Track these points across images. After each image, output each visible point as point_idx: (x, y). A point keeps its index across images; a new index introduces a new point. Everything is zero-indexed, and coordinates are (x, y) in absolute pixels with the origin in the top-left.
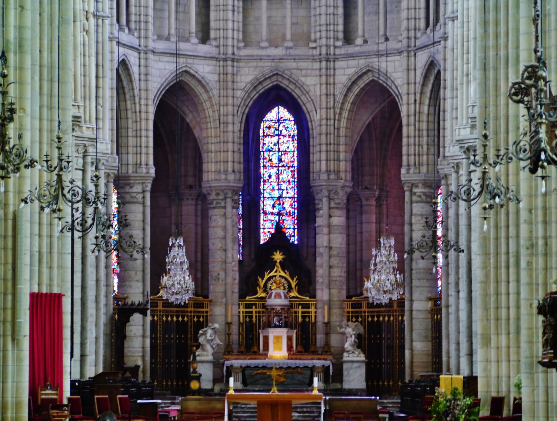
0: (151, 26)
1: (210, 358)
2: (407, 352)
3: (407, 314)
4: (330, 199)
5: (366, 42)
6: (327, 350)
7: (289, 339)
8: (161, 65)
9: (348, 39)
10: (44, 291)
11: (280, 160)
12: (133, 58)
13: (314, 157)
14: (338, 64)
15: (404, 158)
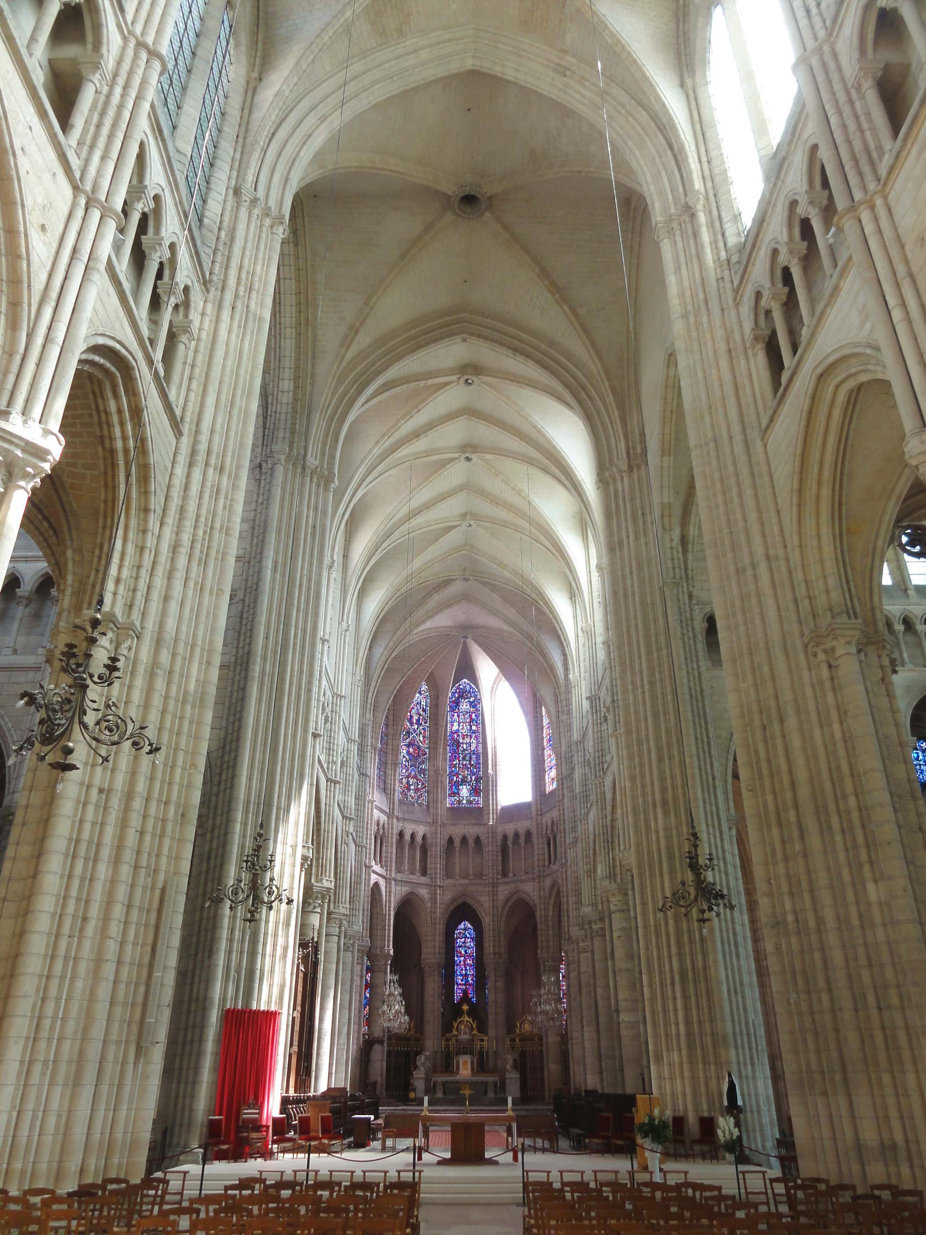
0: (394, 864)
1: (423, 1076)
2: (546, 1072)
3: (544, 1045)
4: (495, 971)
5: (514, 875)
6: (495, 1070)
7: (472, 1063)
8: (399, 888)
9: (505, 874)
10: (262, 1008)
11: (466, 951)
12: (382, 883)
13: (486, 945)
14: (500, 888)
15: (539, 944)
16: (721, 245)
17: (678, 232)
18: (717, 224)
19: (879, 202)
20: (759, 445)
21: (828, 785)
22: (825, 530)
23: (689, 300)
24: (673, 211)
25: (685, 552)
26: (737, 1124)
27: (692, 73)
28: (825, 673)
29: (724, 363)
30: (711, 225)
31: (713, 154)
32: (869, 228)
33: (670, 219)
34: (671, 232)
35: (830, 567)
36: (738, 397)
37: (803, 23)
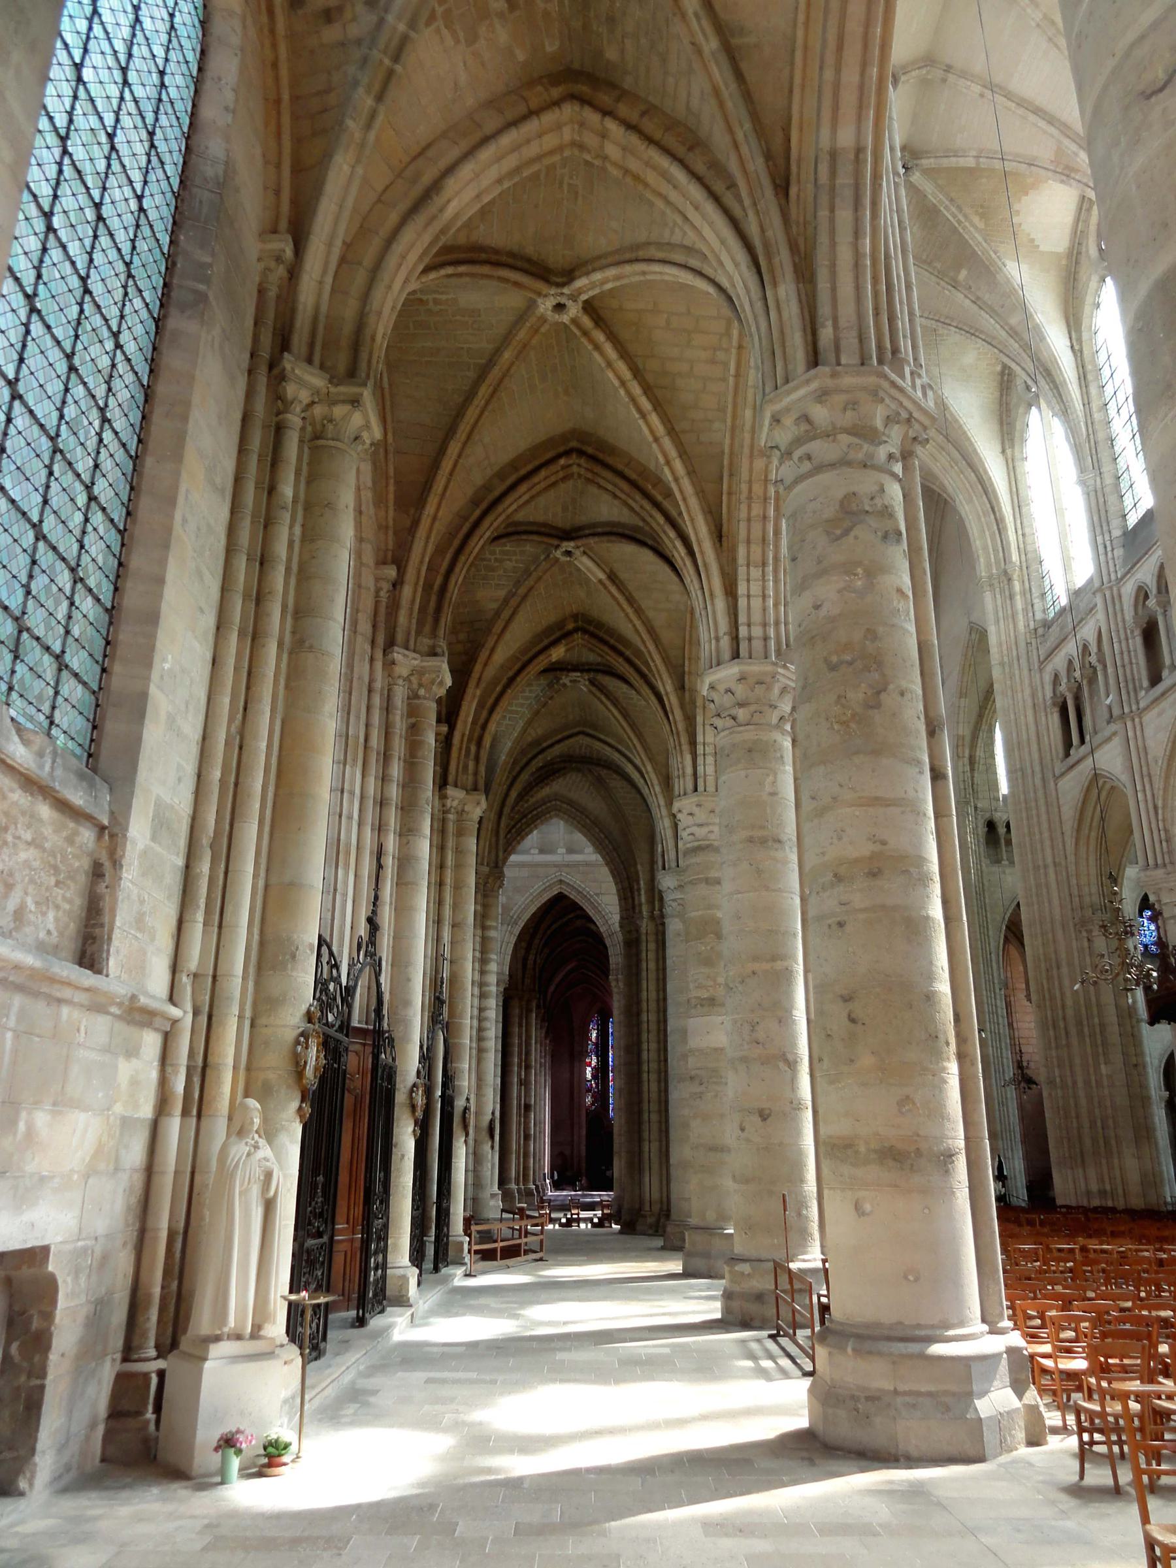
16: (1031, 614)
17: (998, 590)
18: (1028, 596)
19: (1137, 720)
20: (1052, 784)
21: (1083, 1009)
22: (1092, 859)
23: (1005, 652)
24: (994, 571)
25: (972, 770)
26: (1003, 1186)
27: (1012, 446)
28: (1086, 944)
29: (1030, 713)
30: (1023, 593)
31: (1027, 530)
32: (1130, 734)
33: (990, 577)
34: (991, 585)
35: (1093, 879)
36: (1039, 744)
37: (1102, 558)
